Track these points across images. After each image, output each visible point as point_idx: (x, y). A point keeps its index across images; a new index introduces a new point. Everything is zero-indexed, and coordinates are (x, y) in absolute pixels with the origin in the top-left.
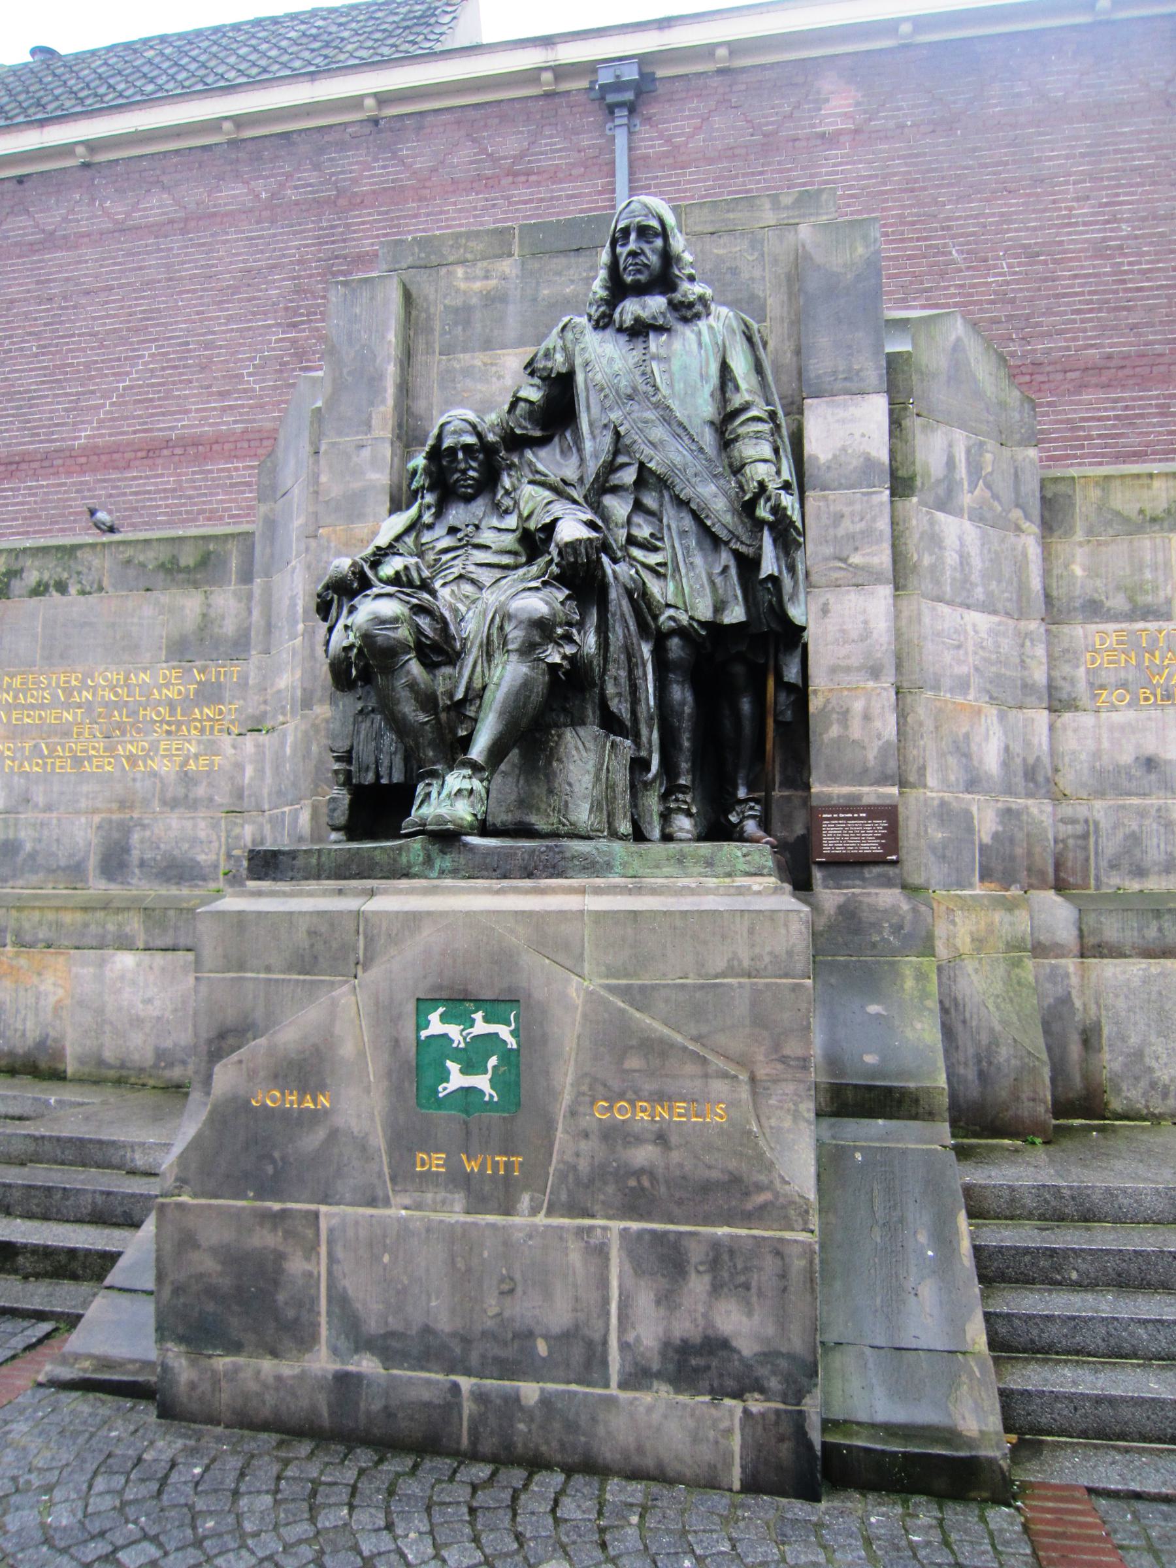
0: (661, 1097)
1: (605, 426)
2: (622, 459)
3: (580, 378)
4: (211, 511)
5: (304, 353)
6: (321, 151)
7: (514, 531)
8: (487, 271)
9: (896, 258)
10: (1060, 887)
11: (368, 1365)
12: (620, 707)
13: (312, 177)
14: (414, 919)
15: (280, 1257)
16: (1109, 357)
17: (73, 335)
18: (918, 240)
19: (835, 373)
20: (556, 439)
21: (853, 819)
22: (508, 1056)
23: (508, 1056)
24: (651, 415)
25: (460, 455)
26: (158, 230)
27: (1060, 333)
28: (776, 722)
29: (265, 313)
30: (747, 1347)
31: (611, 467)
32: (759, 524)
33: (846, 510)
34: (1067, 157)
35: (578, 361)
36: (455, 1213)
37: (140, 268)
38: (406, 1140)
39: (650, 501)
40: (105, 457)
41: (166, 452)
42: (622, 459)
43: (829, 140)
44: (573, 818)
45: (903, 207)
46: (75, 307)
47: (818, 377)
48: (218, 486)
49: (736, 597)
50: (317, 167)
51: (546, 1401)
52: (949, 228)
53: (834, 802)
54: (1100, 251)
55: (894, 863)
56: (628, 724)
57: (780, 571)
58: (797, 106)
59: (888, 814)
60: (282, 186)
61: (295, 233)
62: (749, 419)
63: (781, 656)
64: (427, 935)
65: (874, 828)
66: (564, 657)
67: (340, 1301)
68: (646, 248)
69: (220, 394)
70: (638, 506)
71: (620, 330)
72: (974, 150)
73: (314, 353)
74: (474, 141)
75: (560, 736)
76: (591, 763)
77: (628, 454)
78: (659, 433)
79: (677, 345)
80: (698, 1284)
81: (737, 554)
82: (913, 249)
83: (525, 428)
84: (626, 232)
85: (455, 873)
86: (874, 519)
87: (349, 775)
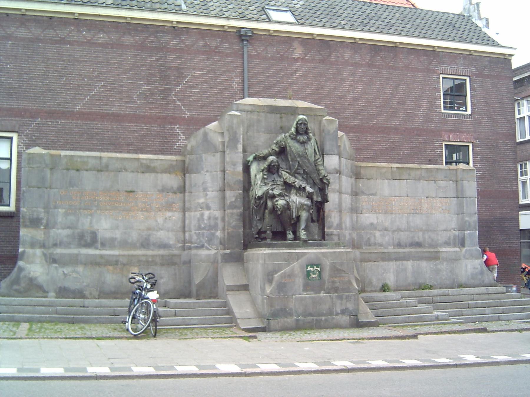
3: (288, 148)
4: (124, 138)
6: (157, 32)
13: (155, 40)
14: (305, 254)
16: (355, 125)
17: (72, 74)
22: (319, 272)
23: (319, 272)
24: (306, 161)
26: (104, 45)
29: (140, 79)
30: (351, 309)
31: (297, 169)
32: (325, 183)
34: (349, 75)
37: (97, 57)
40: (82, 116)
41: (107, 117)
43: (296, 60)
46: (73, 65)
48: (126, 130)
50: (156, 37)
54: (354, 99)
64: (307, 256)
72: (329, 69)
73: (157, 94)
74: (204, 39)
78: (308, 165)
80: (344, 301)
81: (319, 188)
84: (301, 124)
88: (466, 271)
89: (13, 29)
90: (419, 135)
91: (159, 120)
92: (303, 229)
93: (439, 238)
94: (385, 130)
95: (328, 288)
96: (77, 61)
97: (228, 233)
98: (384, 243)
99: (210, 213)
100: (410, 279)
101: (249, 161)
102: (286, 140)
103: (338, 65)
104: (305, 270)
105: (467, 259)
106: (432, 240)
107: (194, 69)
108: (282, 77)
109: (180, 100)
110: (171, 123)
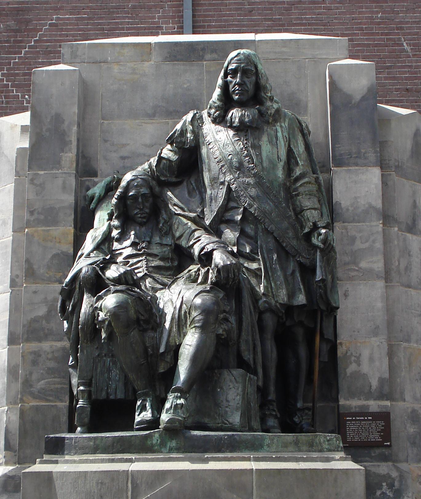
1: (223, 183)
2: (232, 204)
3: (204, 151)
7: (171, 245)
8: (134, 69)
9: (368, 45)
12: (247, 356)
18: (382, 34)
19: (350, 154)
20: (185, 183)
21: (364, 420)
25: (140, 200)
28: (319, 361)
32: (316, 247)
33: (358, 235)
39: (249, 230)
42: (232, 204)
44: (231, 420)
45: (373, 12)
47: (341, 155)
49: (300, 289)
52: (401, 28)
53: (353, 410)
55: (390, 446)
56: (252, 366)
57: (326, 276)
59: (384, 417)
62: (304, 183)
63: (324, 324)
65: (377, 426)
66: (224, 330)
68: (246, 80)
70: (243, 233)
71: (231, 127)
75: (220, 374)
76: (240, 389)
77: (236, 201)
79: (265, 138)
82: (380, 40)
83: (166, 176)
85: (178, 450)
86: (374, 242)
87: (90, 393)
92: (177, 390)
101: (92, 198)
102: (200, 127)
108: (287, 9)
109: (16, 86)
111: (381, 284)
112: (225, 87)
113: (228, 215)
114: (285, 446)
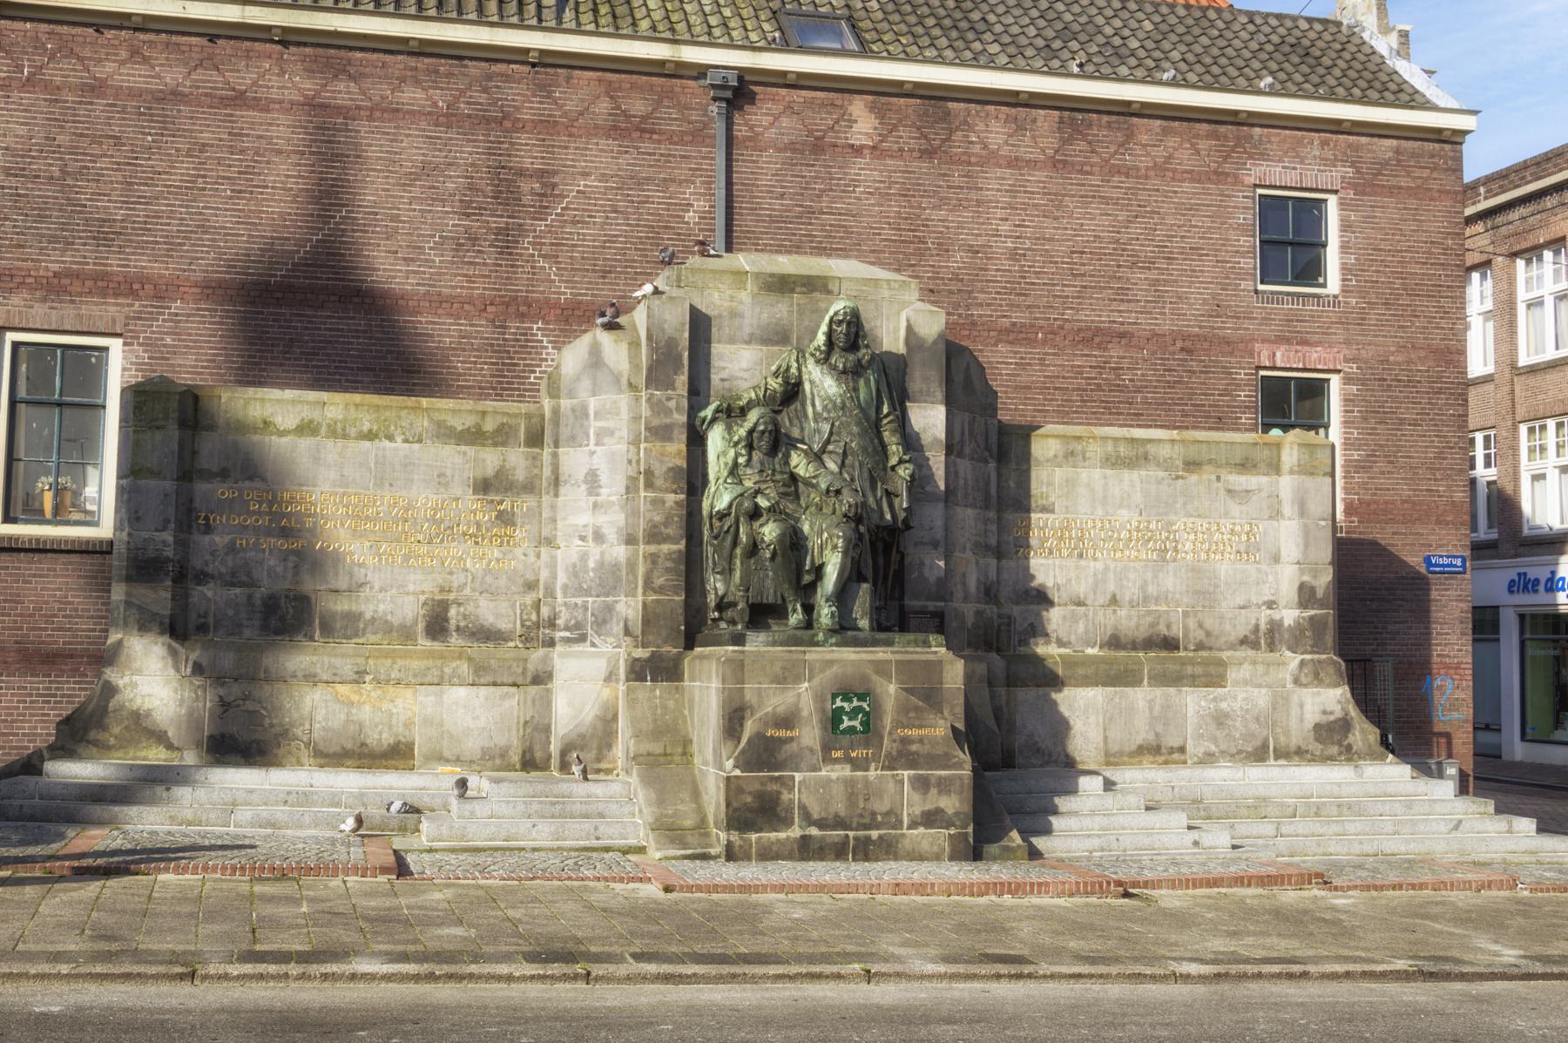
0: (920, 727)
3: (807, 386)
5: (476, 239)
10: (998, 650)
11: (814, 831)
13: (483, 98)
15: (779, 793)
16: (1014, 324)
23: (867, 714)
27: (988, 305)
29: (443, 201)
30: (950, 811)
31: (828, 442)
35: (805, 377)
36: (845, 771)
37: (330, 142)
38: (827, 748)
43: (857, 150)
50: (485, 90)
51: (880, 837)
54: (1013, 255)
58: (837, 122)
60: (457, 99)
61: (469, 141)
67: (803, 808)
69: (404, 259)
74: (612, 98)
80: (934, 791)
88: (1302, 720)
89: (110, 67)
90: (1189, 351)
91: (489, 309)
93: (1228, 627)
94: (1093, 337)
95: (889, 755)
96: (279, 152)
97: (644, 604)
98: (1073, 638)
99: (602, 553)
100: (1143, 735)
103: (969, 163)
104: (829, 707)
105: (1305, 686)
106: (1208, 634)
107: (585, 175)
109: (544, 256)
110: (522, 317)
111: (941, 505)
112: (830, 335)
113: (830, 447)
114: (909, 643)
